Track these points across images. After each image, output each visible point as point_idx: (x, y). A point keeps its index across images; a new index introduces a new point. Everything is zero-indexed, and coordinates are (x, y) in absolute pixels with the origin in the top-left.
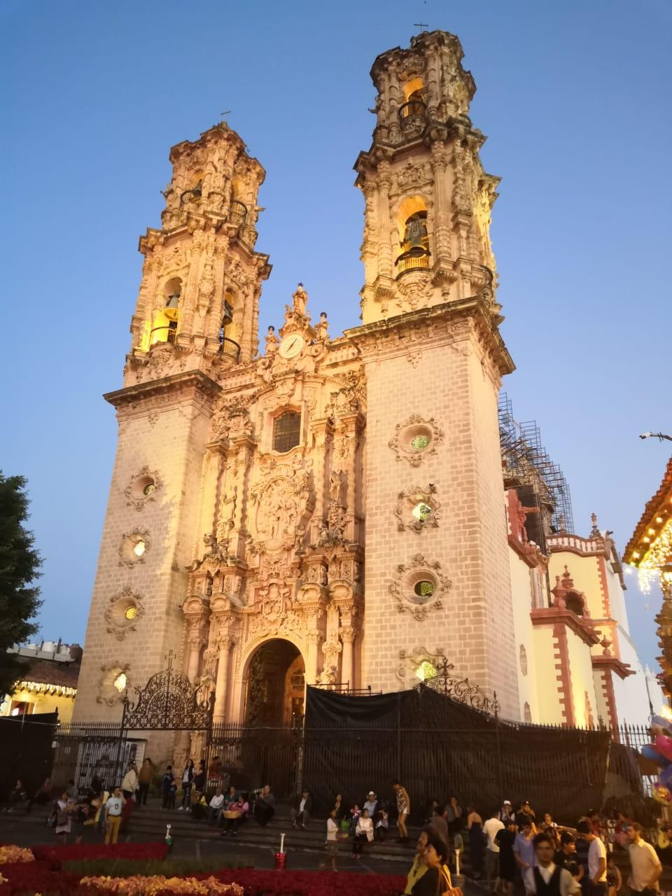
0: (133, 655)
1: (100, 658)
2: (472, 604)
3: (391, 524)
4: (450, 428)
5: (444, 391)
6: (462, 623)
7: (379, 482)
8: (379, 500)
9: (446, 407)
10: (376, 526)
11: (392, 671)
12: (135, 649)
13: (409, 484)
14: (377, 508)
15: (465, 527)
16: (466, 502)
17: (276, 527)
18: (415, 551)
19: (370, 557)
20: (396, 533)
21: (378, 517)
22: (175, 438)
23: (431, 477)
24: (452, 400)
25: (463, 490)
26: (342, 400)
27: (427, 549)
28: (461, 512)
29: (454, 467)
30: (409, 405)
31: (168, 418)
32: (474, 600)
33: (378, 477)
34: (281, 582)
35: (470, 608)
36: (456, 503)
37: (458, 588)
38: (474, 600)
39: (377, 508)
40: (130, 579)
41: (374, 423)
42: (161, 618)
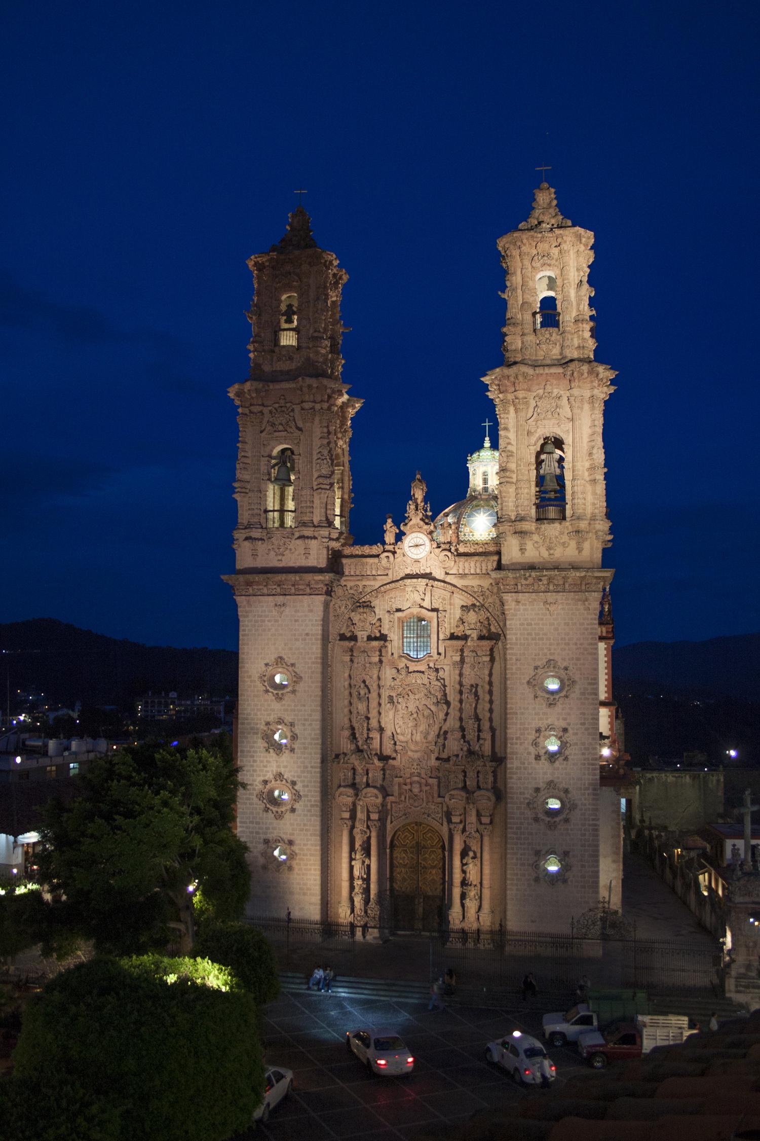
0: (293, 834)
1: (257, 833)
2: (591, 822)
3: (529, 753)
4: (580, 679)
5: (576, 644)
6: (585, 835)
7: (519, 716)
8: (519, 732)
9: (578, 659)
10: (517, 753)
11: (529, 865)
12: (293, 829)
13: (545, 722)
14: (517, 739)
15: (589, 764)
16: (591, 744)
17: (414, 732)
18: (549, 777)
19: (511, 778)
20: (534, 761)
21: (518, 746)
22: (307, 634)
23: (565, 719)
24: (583, 654)
25: (589, 734)
26: (472, 617)
27: (558, 778)
28: (587, 752)
29: (584, 714)
30: (546, 651)
31: (296, 611)
32: (593, 820)
33: (518, 712)
34: (423, 781)
35: (589, 825)
36: (583, 744)
37: (581, 810)
38: (593, 820)
39: (517, 739)
40: (278, 767)
41: (514, 661)
42: (317, 805)
